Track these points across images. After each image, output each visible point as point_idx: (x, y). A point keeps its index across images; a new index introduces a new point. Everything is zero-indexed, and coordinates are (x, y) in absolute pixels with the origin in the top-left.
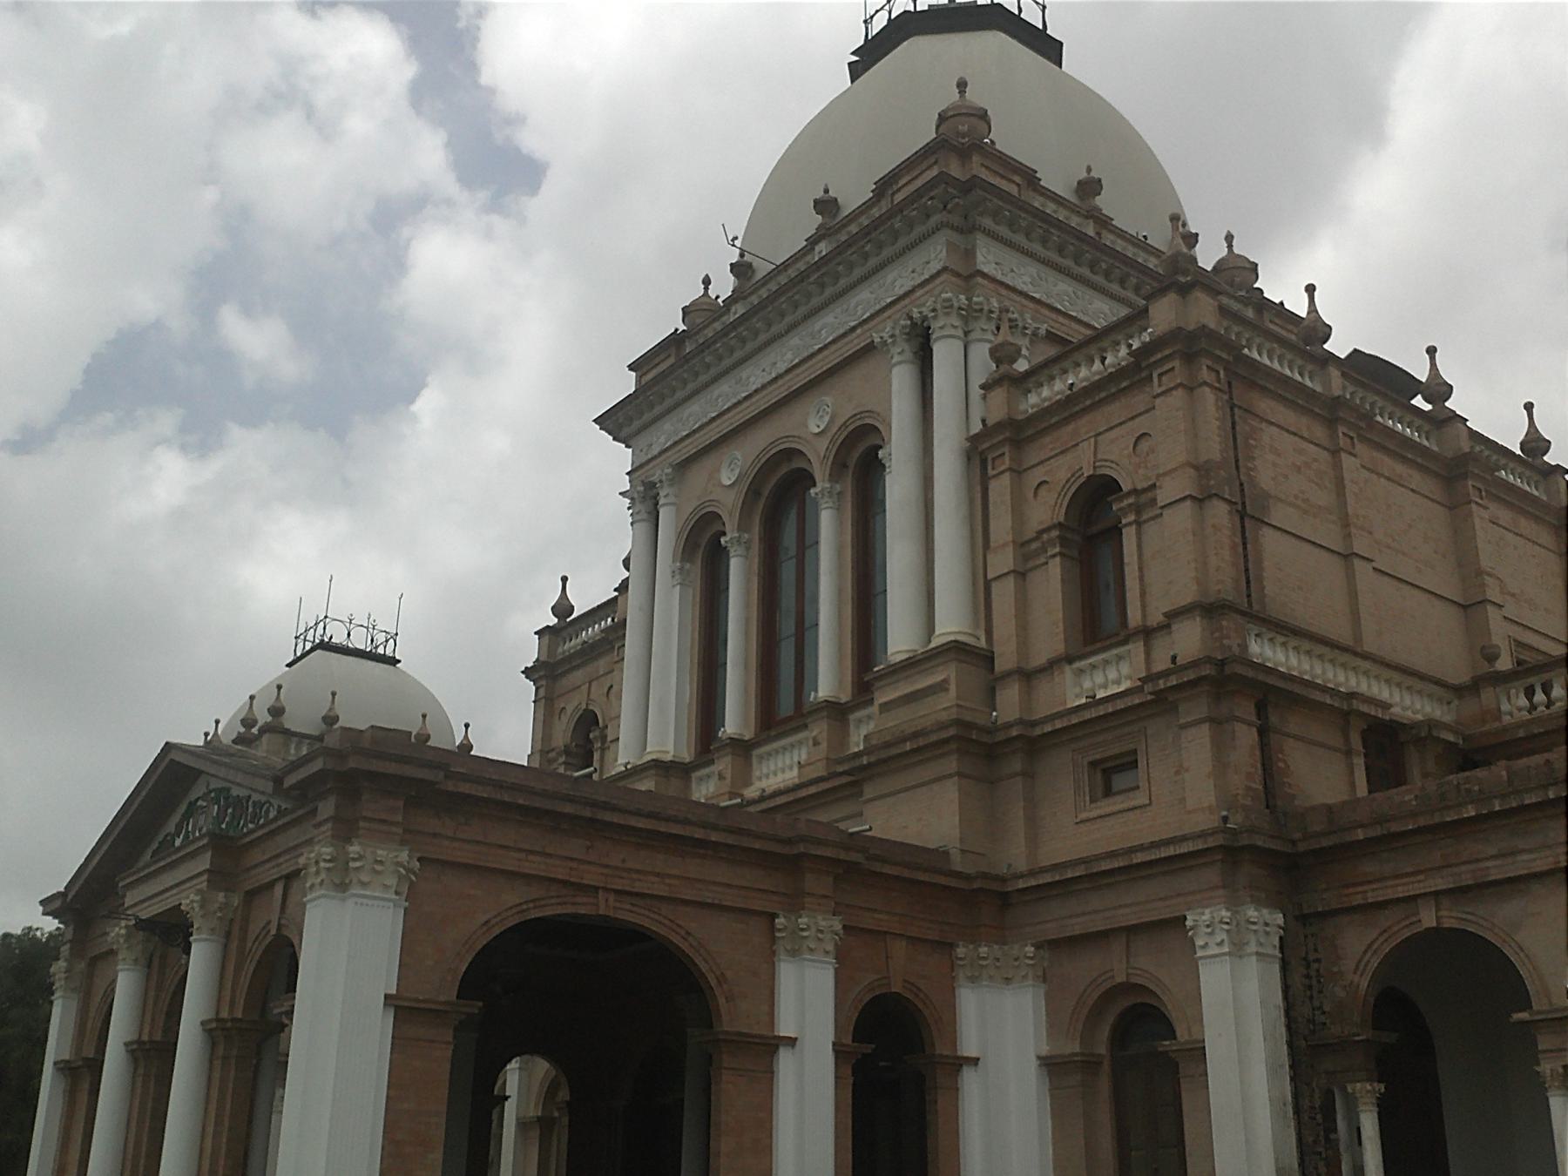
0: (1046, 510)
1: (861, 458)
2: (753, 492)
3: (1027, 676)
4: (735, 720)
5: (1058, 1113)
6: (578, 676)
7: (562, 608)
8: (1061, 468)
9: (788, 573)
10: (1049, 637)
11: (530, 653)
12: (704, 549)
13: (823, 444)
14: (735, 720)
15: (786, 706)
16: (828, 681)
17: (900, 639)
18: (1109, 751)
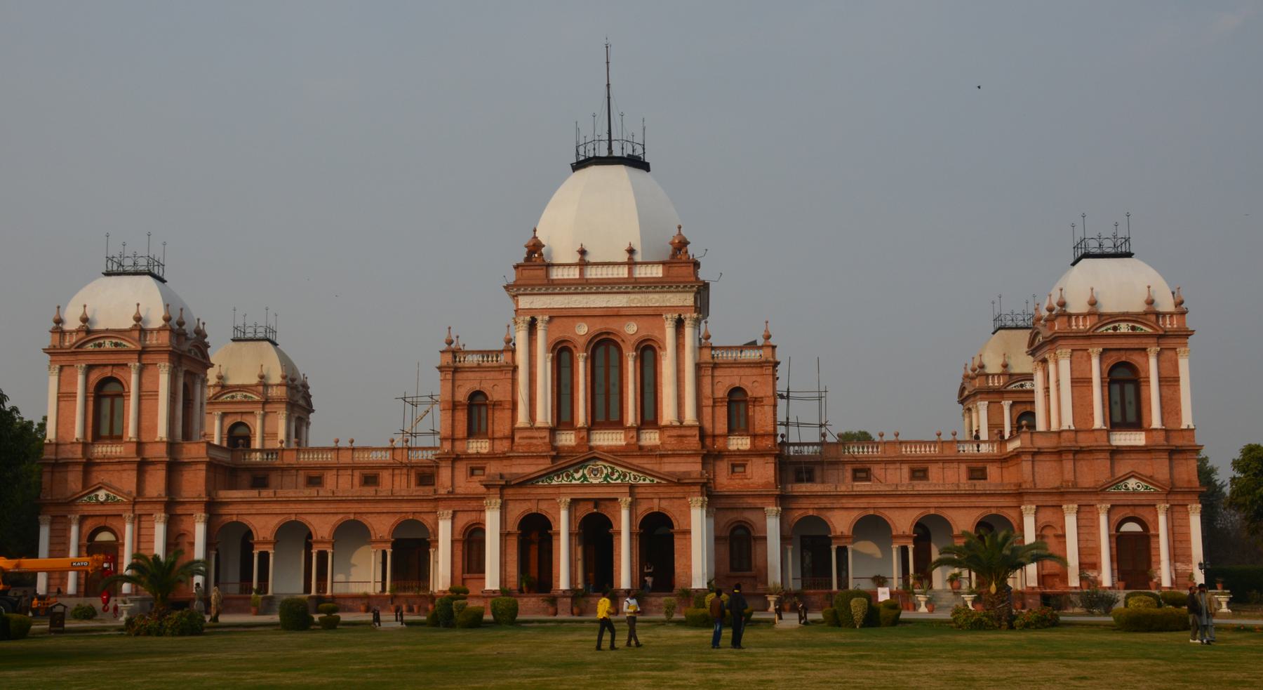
0: (721, 393)
1: (648, 351)
2: (590, 342)
3: (714, 436)
4: (581, 418)
5: (716, 550)
6: (471, 375)
7: (450, 342)
8: (726, 381)
9: (600, 372)
10: (722, 427)
11: (438, 360)
12: (561, 352)
13: (633, 340)
14: (581, 418)
15: (600, 417)
16: (631, 418)
17: (668, 414)
18: (739, 461)
